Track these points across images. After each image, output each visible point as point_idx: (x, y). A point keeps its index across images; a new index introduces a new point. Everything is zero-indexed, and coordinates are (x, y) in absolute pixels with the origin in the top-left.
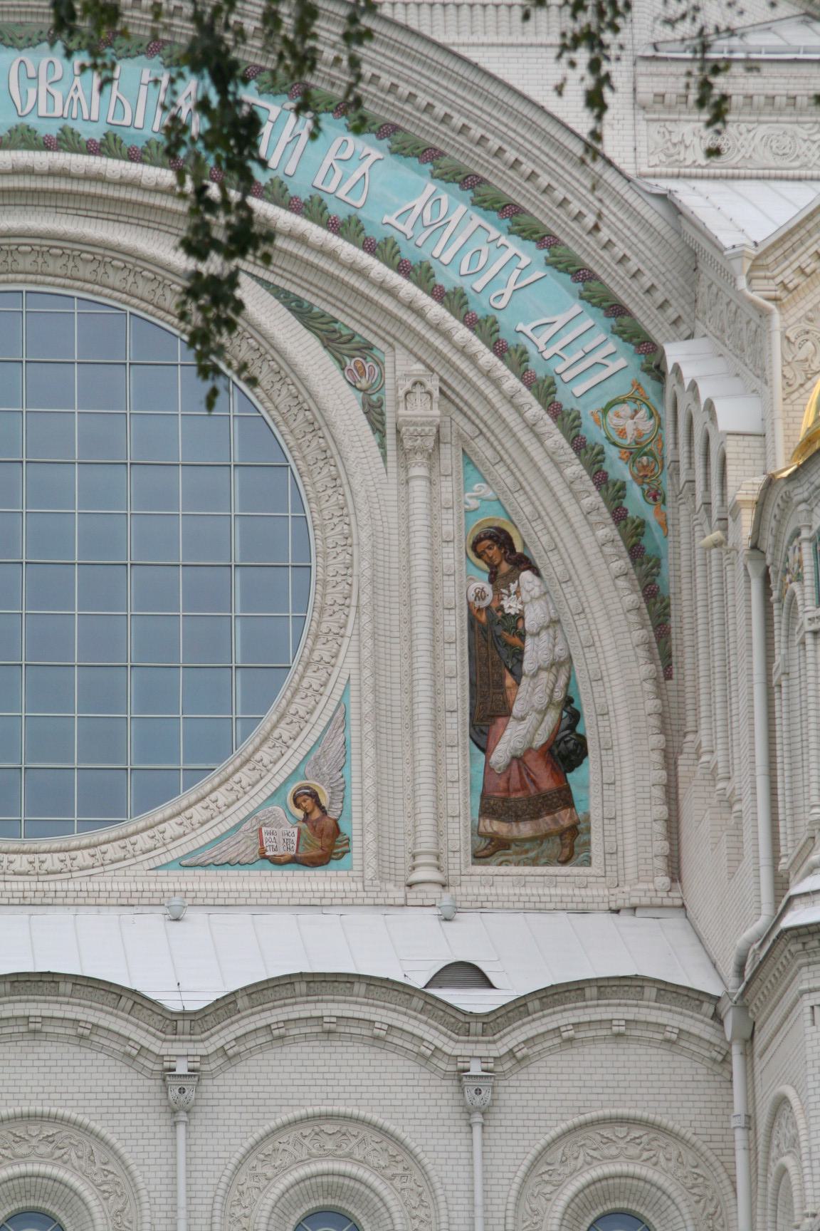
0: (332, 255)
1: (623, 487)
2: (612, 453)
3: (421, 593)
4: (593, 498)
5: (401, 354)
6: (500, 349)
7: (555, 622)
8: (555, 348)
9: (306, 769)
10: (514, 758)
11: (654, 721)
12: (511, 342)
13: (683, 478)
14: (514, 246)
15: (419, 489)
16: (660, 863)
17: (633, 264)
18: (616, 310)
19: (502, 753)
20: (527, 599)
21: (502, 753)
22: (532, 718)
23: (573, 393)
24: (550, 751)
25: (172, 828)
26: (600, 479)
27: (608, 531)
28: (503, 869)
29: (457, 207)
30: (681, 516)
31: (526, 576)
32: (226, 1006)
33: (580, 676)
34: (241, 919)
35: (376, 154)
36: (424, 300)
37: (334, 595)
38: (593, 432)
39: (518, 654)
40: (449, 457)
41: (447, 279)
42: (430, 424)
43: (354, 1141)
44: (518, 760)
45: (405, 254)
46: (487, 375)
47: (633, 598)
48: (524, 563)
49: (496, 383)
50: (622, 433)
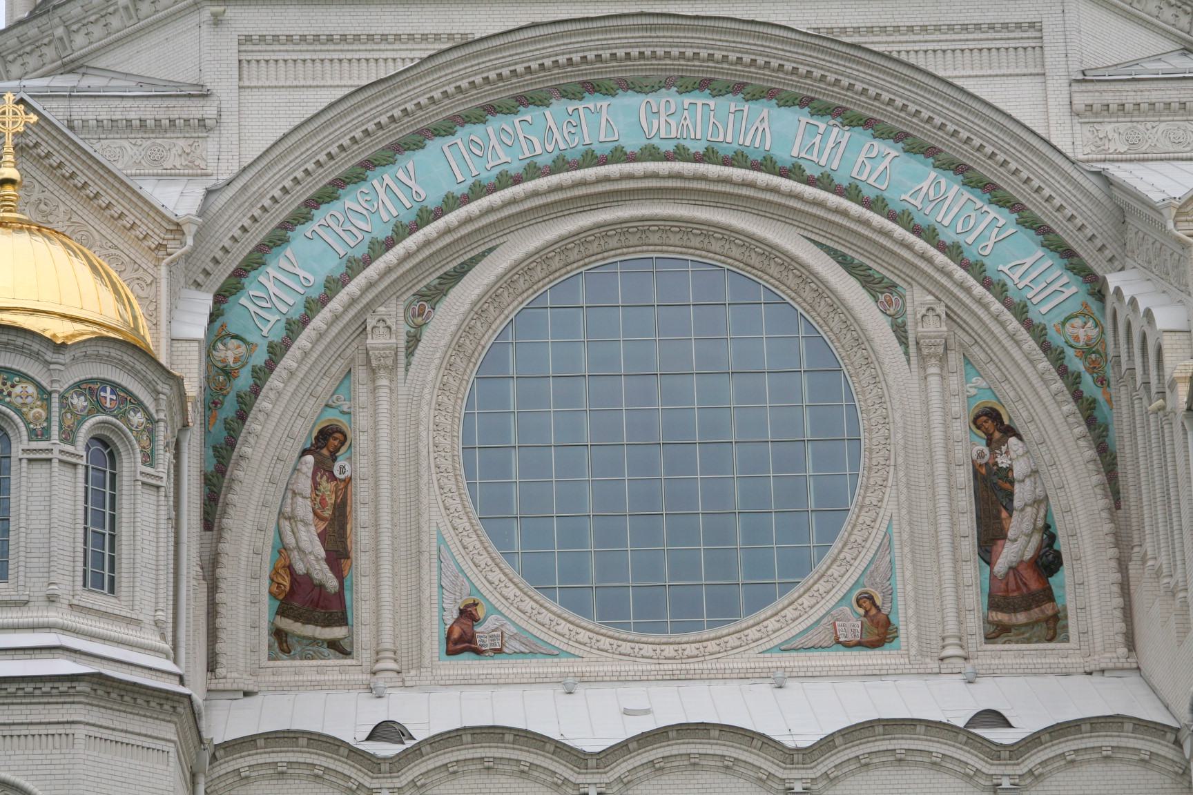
0: (866, 223)
1: (1079, 376)
2: (1070, 352)
3: (939, 455)
4: (1059, 385)
5: (917, 290)
6: (987, 284)
7: (1035, 472)
8: (1026, 281)
9: (865, 580)
10: (1010, 568)
11: (1110, 539)
12: (995, 278)
13: (1124, 367)
14: (993, 212)
15: (934, 382)
16: (1120, 638)
17: (1079, 221)
18: (1067, 253)
19: (1001, 565)
20: (1014, 457)
21: (1001, 565)
22: (1022, 540)
23: (1041, 311)
24: (1036, 562)
25: (772, 624)
26: (1063, 371)
27: (1070, 407)
28: (1007, 646)
29: (952, 187)
30: (1122, 395)
31: (1013, 440)
32: (827, 744)
33: (1054, 509)
34: (824, 685)
35: (894, 153)
36: (932, 252)
37: (878, 459)
38: (1056, 339)
39: (1010, 495)
40: (954, 359)
41: (947, 237)
42: (940, 337)
44: (1013, 569)
45: (917, 221)
46: (979, 301)
47: (1090, 453)
48: (1010, 431)
49: (986, 307)
50: (1077, 338)
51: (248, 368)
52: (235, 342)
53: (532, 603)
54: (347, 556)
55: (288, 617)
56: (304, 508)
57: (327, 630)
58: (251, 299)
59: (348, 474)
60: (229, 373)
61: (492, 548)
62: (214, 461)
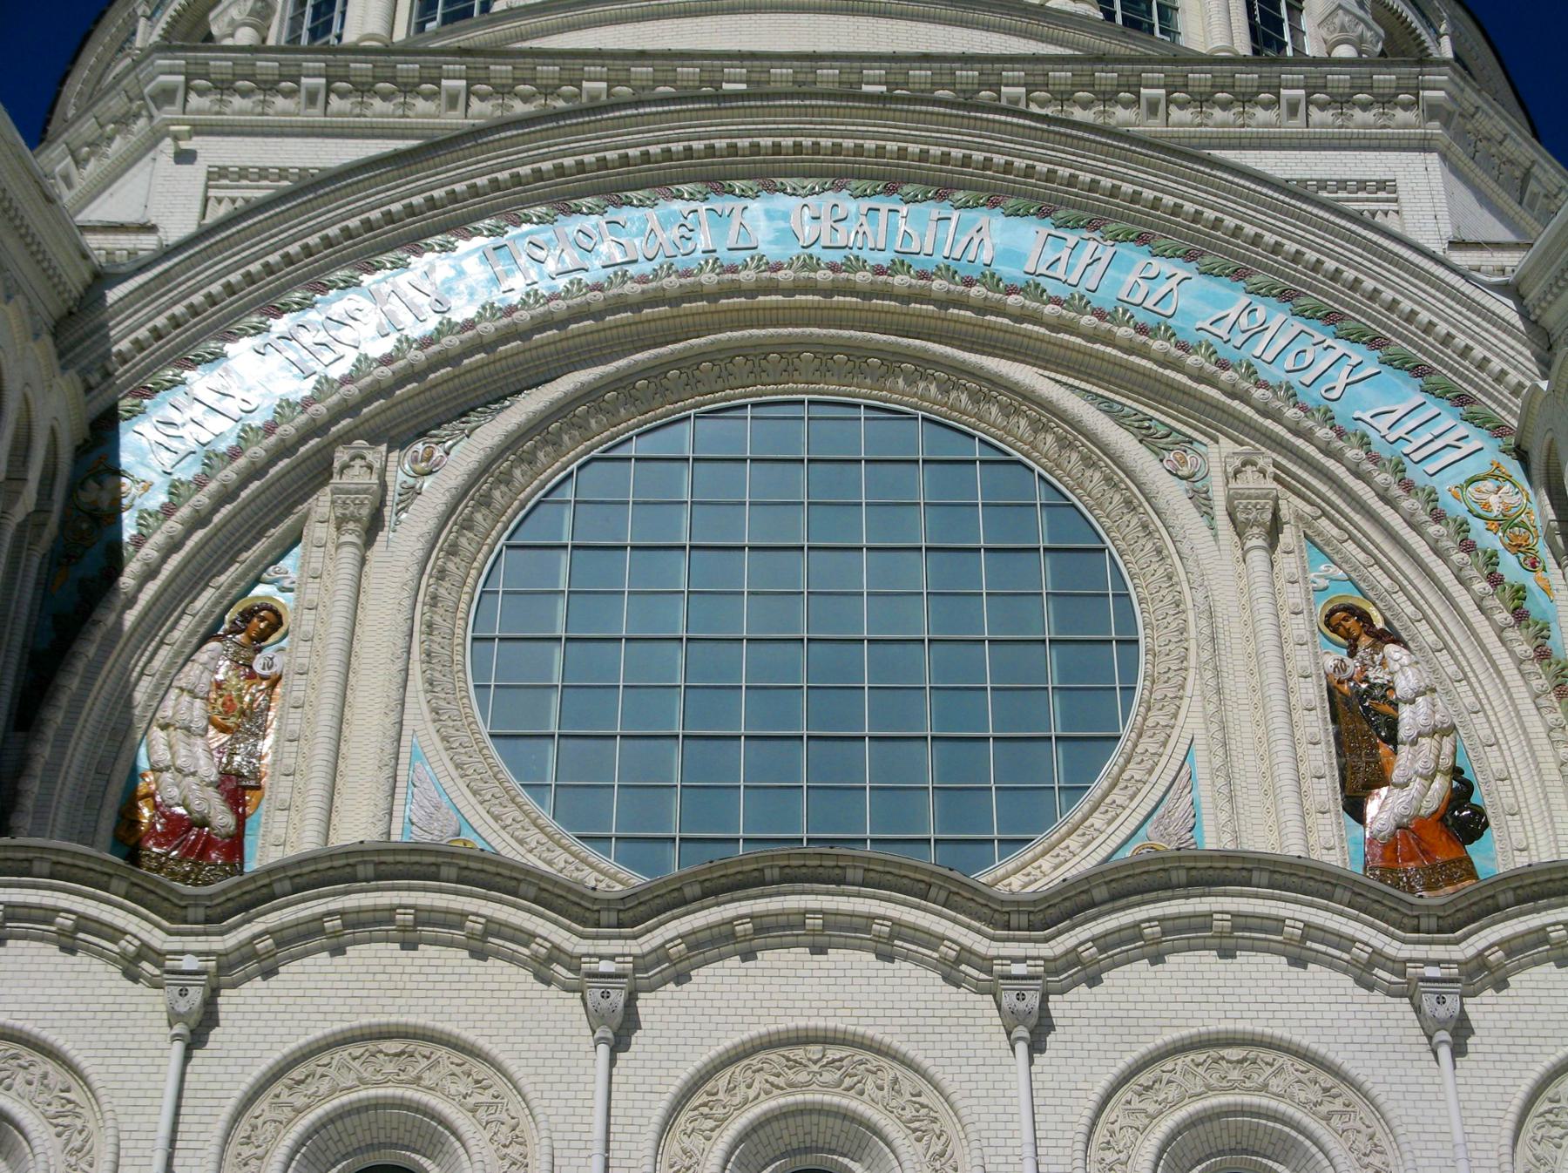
1: (1494, 554)
2: (1477, 525)
8: (1400, 431)
12: (1349, 427)
24: (1442, 819)
31: (1391, 649)
39: (1393, 724)
43: (1269, 1070)
50: (1487, 506)
53: (567, 855)
61: (507, 774)
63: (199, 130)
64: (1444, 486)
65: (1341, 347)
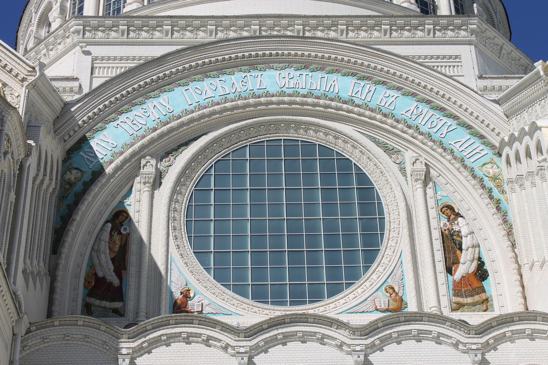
1: (491, 189)
2: (486, 179)
10: (463, 277)
12: (448, 147)
22: (468, 263)
24: (476, 274)
26: (483, 187)
28: (463, 313)
31: (460, 219)
39: (460, 244)
42: (422, 171)
48: (458, 215)
50: (489, 173)
51: (81, 182)
52: (76, 171)
54: (125, 268)
55: (93, 297)
56: (104, 246)
57: (112, 303)
58: (85, 152)
59: (128, 231)
60: (71, 184)
62: (61, 223)
63: (89, 44)
64: (476, 166)
65: (445, 119)
